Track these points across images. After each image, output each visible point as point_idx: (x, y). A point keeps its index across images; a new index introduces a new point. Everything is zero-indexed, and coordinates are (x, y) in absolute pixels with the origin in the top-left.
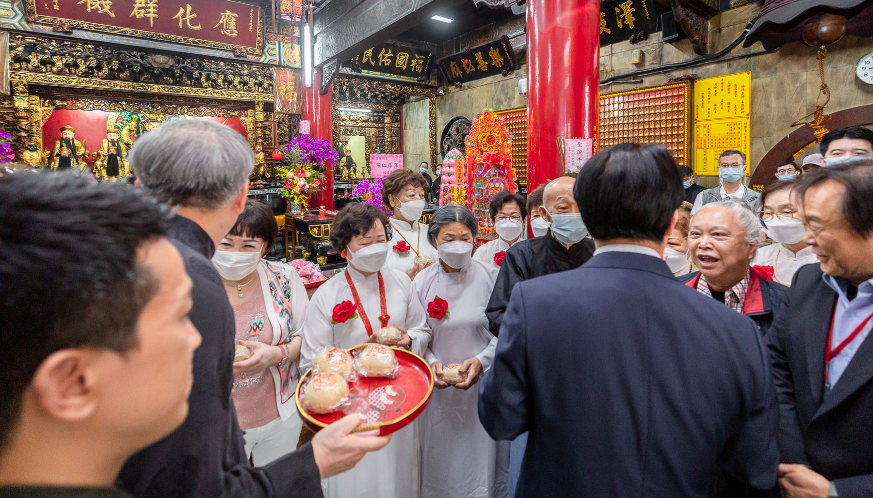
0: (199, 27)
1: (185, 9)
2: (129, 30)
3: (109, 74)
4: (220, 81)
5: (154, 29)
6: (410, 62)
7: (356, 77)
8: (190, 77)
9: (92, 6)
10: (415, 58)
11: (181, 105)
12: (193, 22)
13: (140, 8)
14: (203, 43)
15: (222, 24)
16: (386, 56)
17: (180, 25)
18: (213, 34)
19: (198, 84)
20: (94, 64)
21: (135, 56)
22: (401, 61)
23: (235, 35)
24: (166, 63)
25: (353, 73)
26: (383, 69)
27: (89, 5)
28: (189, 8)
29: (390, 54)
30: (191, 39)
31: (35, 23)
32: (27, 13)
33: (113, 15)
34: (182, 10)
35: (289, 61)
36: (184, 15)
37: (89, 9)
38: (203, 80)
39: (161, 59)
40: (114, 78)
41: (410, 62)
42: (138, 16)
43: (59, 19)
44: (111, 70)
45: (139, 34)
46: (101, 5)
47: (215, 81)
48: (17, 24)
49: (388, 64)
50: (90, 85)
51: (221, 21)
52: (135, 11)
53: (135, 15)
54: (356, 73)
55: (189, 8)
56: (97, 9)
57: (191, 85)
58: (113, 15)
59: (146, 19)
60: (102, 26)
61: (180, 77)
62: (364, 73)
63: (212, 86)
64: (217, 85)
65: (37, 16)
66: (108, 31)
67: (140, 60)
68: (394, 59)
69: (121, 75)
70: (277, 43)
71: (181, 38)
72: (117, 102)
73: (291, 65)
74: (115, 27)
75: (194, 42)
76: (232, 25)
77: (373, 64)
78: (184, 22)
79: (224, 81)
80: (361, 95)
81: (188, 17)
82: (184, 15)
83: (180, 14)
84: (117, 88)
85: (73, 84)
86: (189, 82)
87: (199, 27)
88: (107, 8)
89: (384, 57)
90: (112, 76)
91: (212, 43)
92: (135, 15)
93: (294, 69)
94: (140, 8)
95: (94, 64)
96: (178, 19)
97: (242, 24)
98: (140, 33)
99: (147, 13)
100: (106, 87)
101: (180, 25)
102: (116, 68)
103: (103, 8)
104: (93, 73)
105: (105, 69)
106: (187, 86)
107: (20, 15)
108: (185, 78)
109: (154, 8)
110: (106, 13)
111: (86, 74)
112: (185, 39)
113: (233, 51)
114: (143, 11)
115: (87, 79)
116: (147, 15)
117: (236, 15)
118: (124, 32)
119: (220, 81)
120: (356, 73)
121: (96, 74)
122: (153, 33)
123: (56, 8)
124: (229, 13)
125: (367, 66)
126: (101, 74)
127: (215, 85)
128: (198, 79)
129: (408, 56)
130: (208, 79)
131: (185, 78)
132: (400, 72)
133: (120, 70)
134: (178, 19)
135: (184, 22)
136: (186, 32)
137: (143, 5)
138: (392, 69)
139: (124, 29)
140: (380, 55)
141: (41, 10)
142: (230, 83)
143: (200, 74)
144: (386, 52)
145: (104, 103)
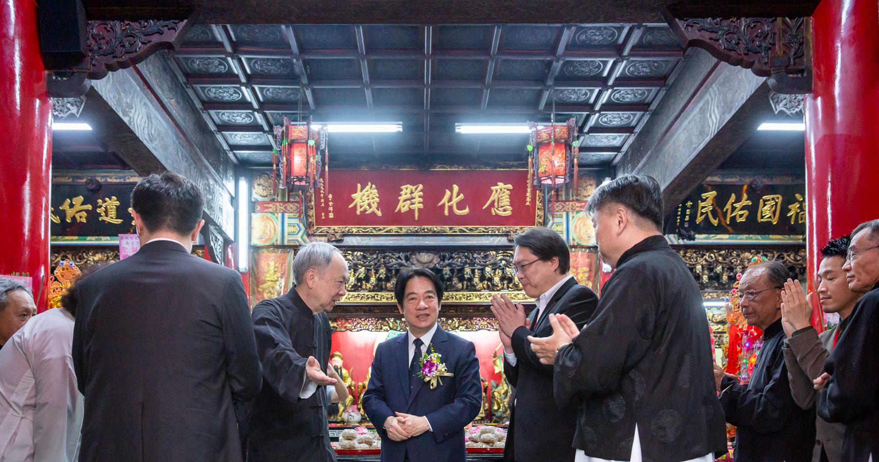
0: (466, 211)
1: (451, 191)
2: (394, 228)
3: (377, 285)
4: (497, 279)
5: (420, 222)
6: (785, 210)
7: (686, 247)
8: (461, 279)
9: (361, 207)
10: (795, 201)
11: (451, 318)
12: (460, 206)
13: (405, 201)
14: (471, 230)
15: (493, 202)
16: (737, 205)
17: (446, 212)
18: (482, 216)
19: (472, 288)
20: (362, 276)
21: (399, 258)
22: (767, 211)
23: (508, 213)
24: (431, 262)
25: (681, 242)
26: (737, 228)
27: (358, 207)
28: (456, 188)
29: (745, 202)
30: (457, 228)
31: (314, 235)
32: (309, 226)
33: (379, 213)
34: (448, 193)
35: (581, 238)
36: (450, 200)
37: (358, 212)
38: (476, 280)
39: (425, 257)
40: (381, 289)
41: (785, 210)
42: (404, 210)
43: (333, 227)
44: (379, 280)
45: (404, 231)
46: (369, 205)
47: (490, 280)
48: (300, 240)
49: (743, 220)
50: (358, 300)
51: (491, 199)
52: (401, 204)
53: (400, 210)
54: (687, 242)
55: (456, 188)
56: (365, 210)
57: (462, 289)
58: (379, 213)
59: (411, 211)
60: (369, 228)
61: (450, 279)
62: (701, 239)
63: (488, 288)
64: (493, 285)
65: (315, 227)
66: (375, 233)
67: (404, 262)
68: (753, 210)
69: (389, 285)
70: (564, 214)
71: (447, 228)
72: (383, 319)
73: (584, 244)
74: (381, 227)
75: (461, 231)
76: (506, 201)
77: (715, 222)
78: (451, 208)
79: (502, 279)
80: (710, 278)
81: (455, 200)
82: (450, 200)
83: (445, 200)
84: (384, 300)
85: (342, 301)
86: (460, 285)
87: (466, 211)
88: (374, 206)
89: (734, 209)
90: (379, 287)
91: (481, 228)
92: (400, 210)
93: (589, 248)
94: (405, 201)
95: (362, 276)
96: (444, 205)
97: (517, 197)
98: (405, 229)
99: (412, 204)
100: (373, 301)
101: (446, 212)
102: (383, 276)
103: (370, 207)
104: (361, 287)
105: (373, 280)
106: (457, 290)
107: (303, 228)
108: (455, 280)
109: (420, 197)
110: (373, 213)
111: (355, 288)
112: (451, 229)
113: (506, 234)
114: (408, 202)
115: (355, 294)
116: (412, 207)
117: (510, 186)
118: (389, 231)
119: (497, 279)
120: (687, 242)
121: (364, 287)
122: (417, 227)
123: (331, 216)
124: (501, 185)
125: (708, 228)
126: (369, 285)
127: (492, 287)
128: (470, 280)
129: (780, 201)
130: (482, 278)
131: (455, 280)
132: (766, 229)
133: (388, 279)
134: (444, 205)
135: (451, 208)
136: (454, 220)
137: (409, 196)
138: (752, 226)
139: (389, 228)
140: (728, 206)
141: (319, 222)
142: (510, 280)
143: (473, 271)
144: (738, 200)
145: (370, 323)
